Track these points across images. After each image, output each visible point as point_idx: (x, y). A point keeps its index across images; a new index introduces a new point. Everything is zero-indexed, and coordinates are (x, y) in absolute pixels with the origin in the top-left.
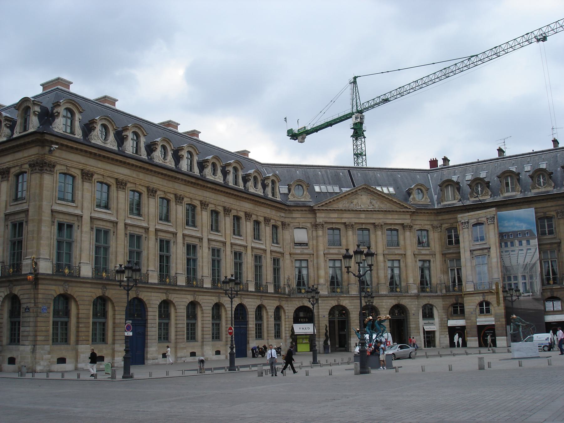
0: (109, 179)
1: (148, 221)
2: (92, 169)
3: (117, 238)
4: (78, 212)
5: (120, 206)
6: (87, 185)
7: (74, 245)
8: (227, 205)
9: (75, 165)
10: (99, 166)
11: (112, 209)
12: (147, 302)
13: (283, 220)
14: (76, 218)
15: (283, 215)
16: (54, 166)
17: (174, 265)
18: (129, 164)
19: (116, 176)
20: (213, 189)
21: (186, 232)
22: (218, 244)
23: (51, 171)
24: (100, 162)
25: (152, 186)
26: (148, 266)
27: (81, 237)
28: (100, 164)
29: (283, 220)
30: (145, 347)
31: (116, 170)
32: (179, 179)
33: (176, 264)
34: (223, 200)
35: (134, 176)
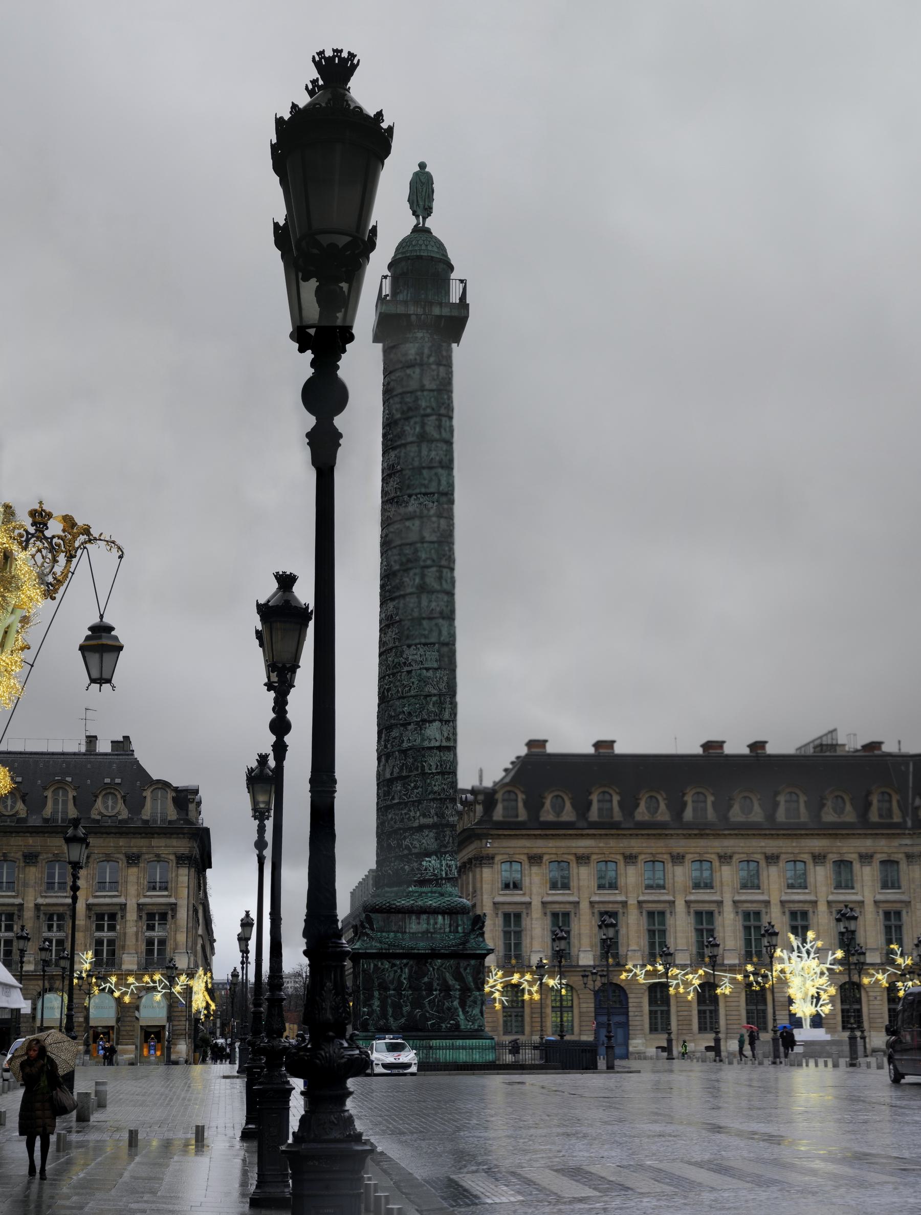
0: (566, 856)
1: (627, 893)
2: (539, 851)
3: (579, 919)
4: (526, 899)
5: (582, 883)
6: (535, 869)
7: (523, 934)
8: (769, 851)
9: (518, 850)
10: (550, 845)
11: (571, 888)
12: (626, 988)
13: (909, 850)
14: (524, 906)
15: (908, 842)
16: (493, 858)
17: (672, 940)
18: (588, 835)
19: (574, 851)
20: (736, 835)
21: (692, 898)
22: (755, 905)
23: (490, 864)
24: (551, 841)
25: (628, 852)
26: (628, 946)
27: (531, 924)
28: (551, 843)
29: (906, 851)
30: (628, 1039)
31: (574, 845)
32: (672, 835)
33: (676, 938)
34: (763, 844)
35: (601, 845)
